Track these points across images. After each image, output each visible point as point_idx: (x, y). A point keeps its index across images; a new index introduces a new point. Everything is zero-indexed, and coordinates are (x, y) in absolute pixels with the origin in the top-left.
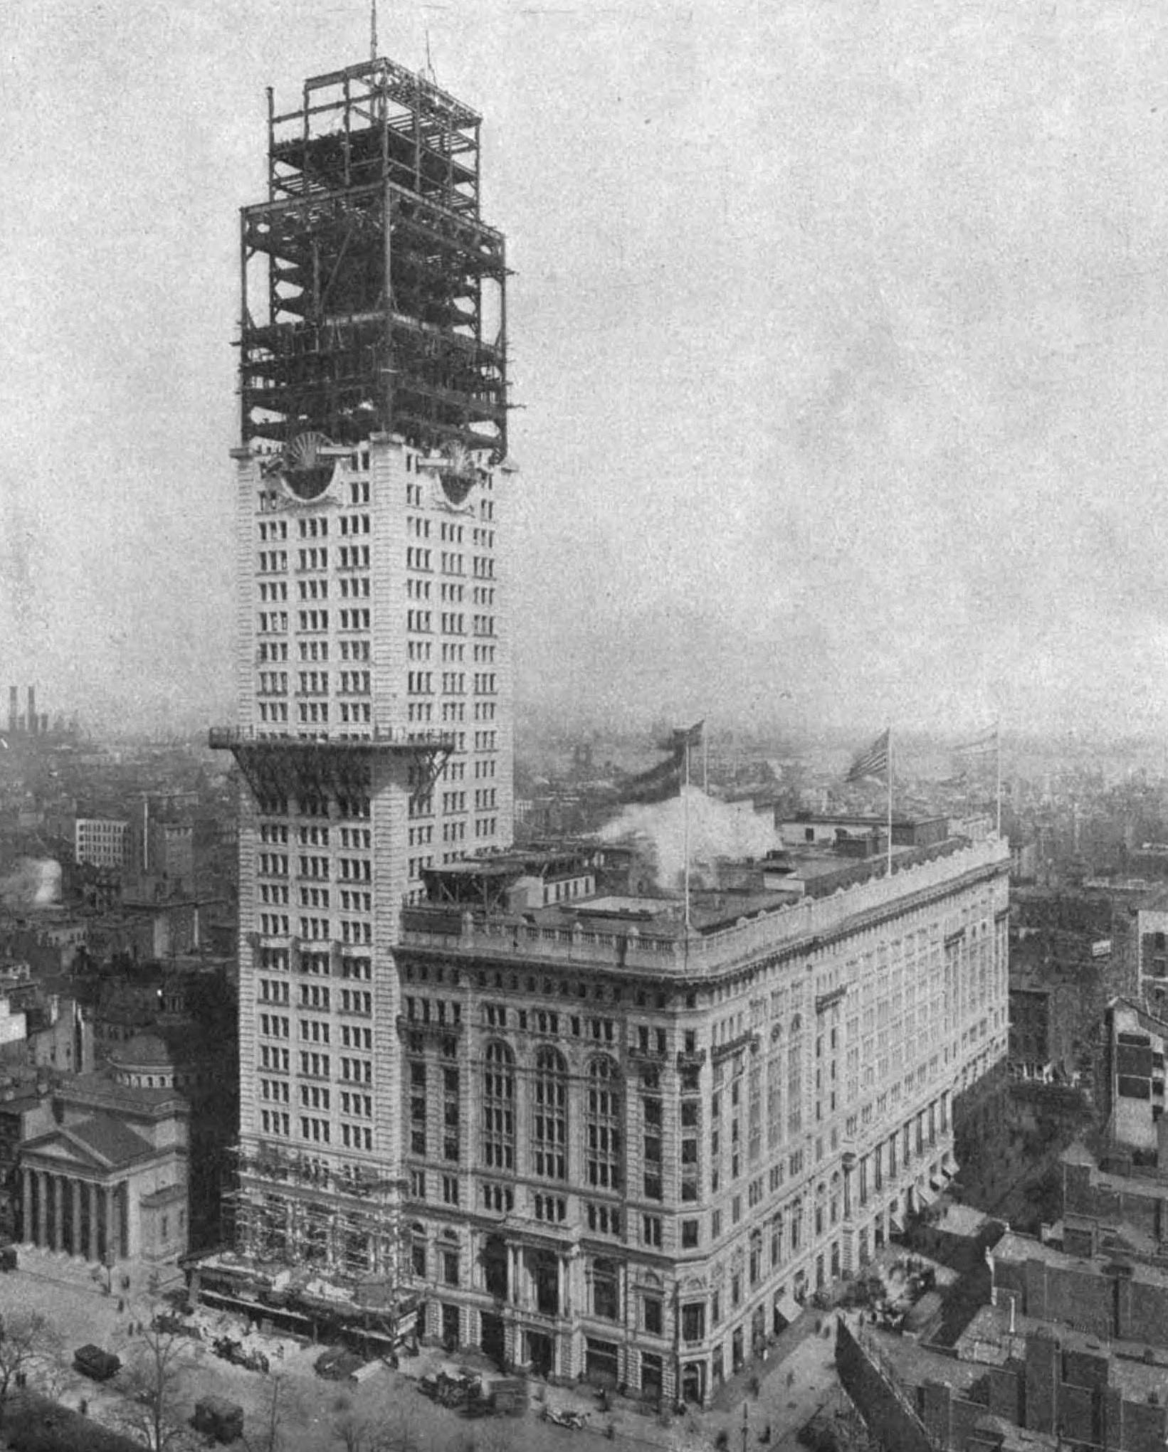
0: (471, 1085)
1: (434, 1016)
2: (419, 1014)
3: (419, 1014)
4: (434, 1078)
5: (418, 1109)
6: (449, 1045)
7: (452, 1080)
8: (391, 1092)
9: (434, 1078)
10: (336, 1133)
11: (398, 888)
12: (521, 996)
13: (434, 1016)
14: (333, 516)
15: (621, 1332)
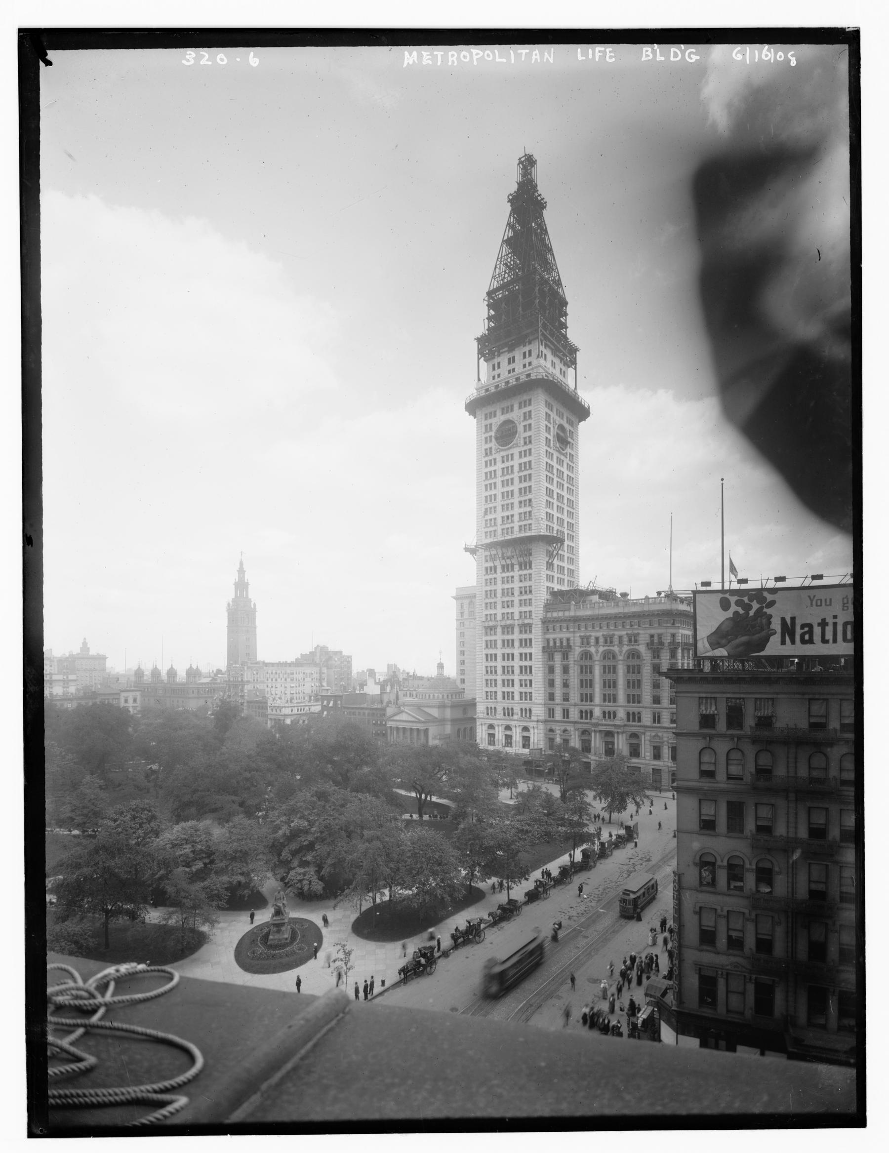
0: (574, 671)
1: (558, 644)
2: (551, 644)
3: (551, 644)
4: (558, 670)
5: (551, 683)
6: (565, 657)
7: (566, 670)
8: (538, 677)
9: (558, 670)
10: (517, 697)
11: (541, 596)
12: (597, 631)
13: (558, 644)
14: (516, 451)
15: (643, 761)
